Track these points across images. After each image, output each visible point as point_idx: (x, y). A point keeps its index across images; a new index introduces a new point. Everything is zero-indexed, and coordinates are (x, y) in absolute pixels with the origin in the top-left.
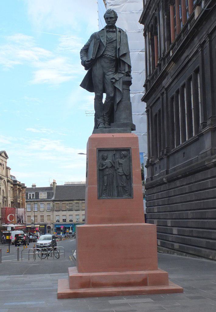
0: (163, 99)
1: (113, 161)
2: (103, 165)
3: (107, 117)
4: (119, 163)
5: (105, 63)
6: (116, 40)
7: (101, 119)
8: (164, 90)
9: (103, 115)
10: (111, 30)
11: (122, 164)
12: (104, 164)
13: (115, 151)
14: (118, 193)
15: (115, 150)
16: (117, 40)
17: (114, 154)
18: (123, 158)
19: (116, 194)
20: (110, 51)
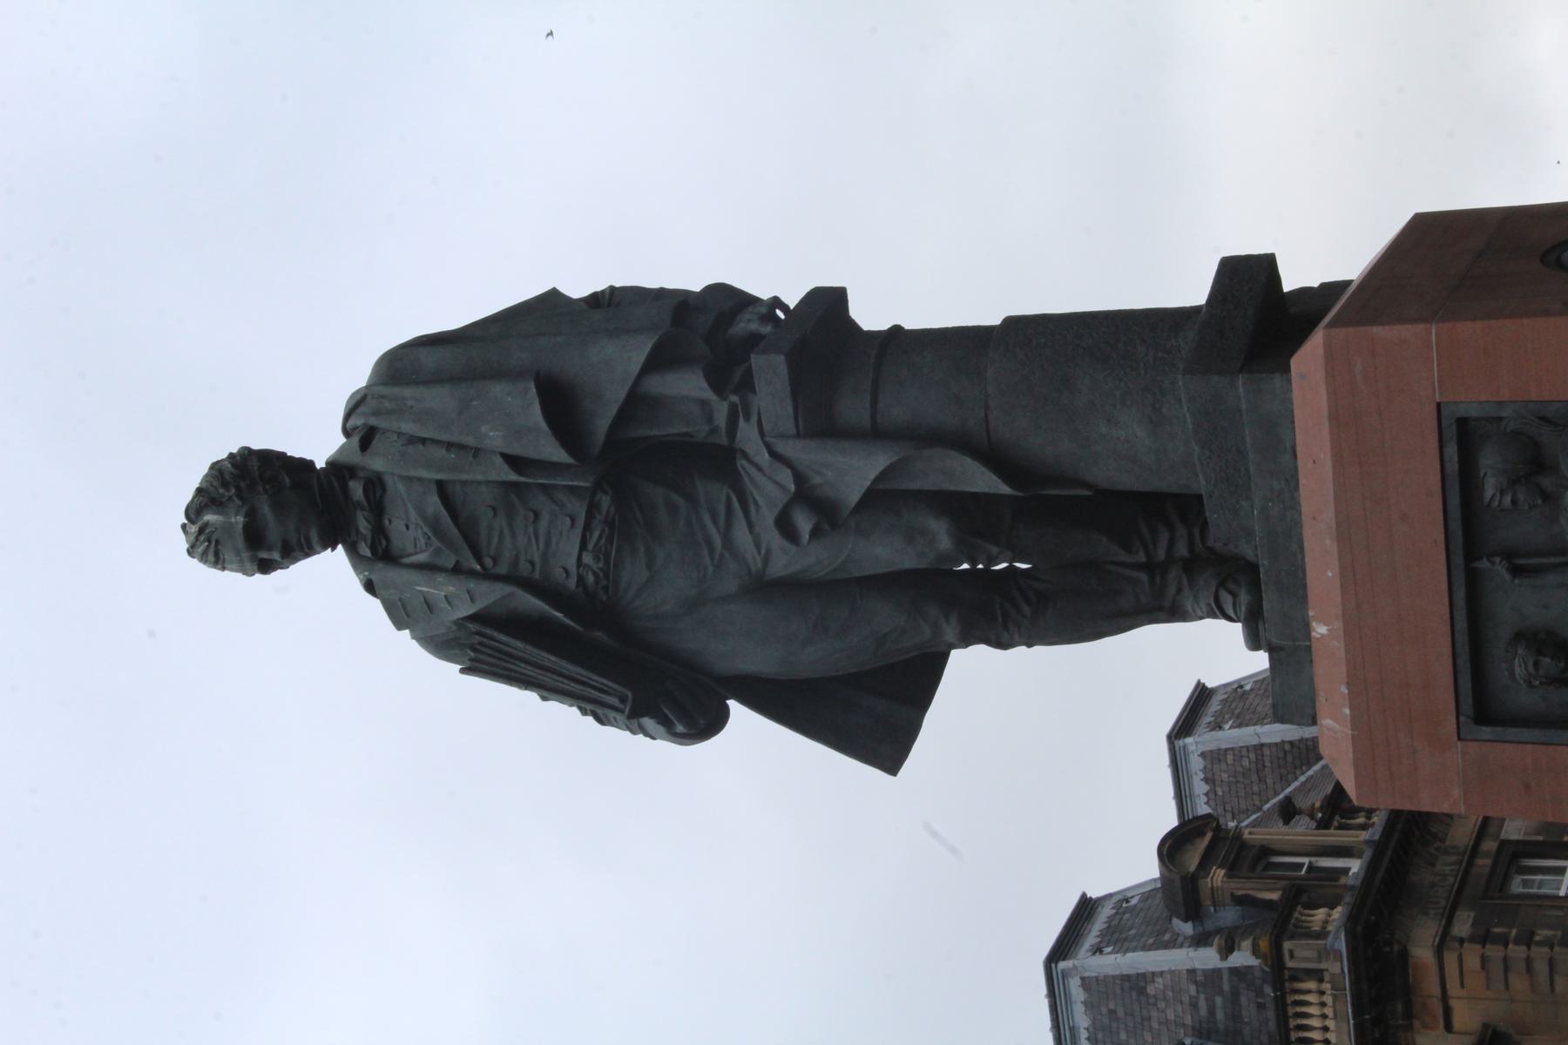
3: (1164, 538)
5: (658, 587)
6: (441, 486)
7: (1179, 591)
9: (1144, 577)
10: (363, 525)
15: (1471, 555)
16: (439, 477)
17: (1516, 571)
18: (1547, 482)
20: (548, 544)
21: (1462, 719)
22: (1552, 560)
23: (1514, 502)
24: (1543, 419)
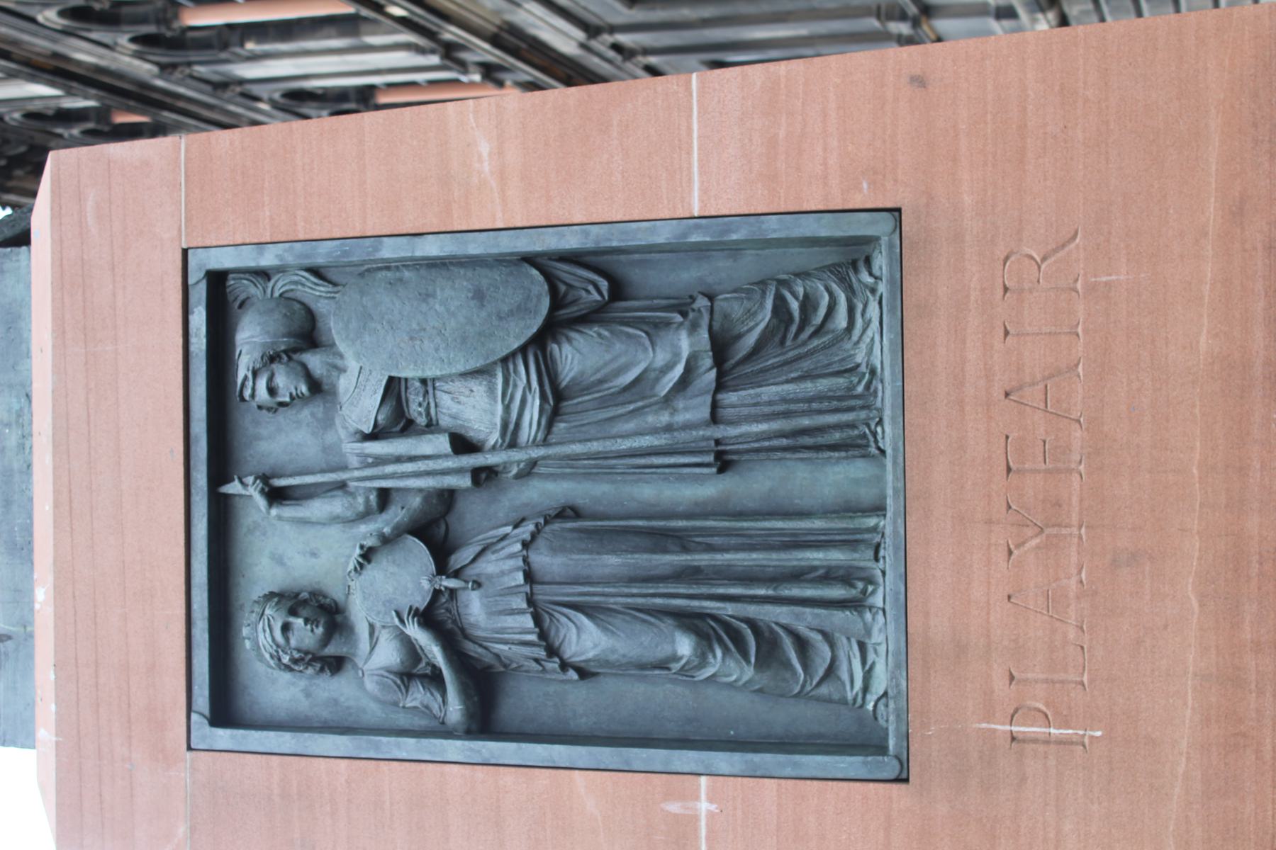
0: (647, 51)
1: (364, 516)
2: (413, 671)
4: (376, 434)
8: (594, 44)
11: (394, 389)
12: (388, 654)
13: (233, 488)
14: (805, 443)
19: (835, 478)
21: (194, 717)
22: (319, 478)
23: (272, 391)
24: (316, 271)
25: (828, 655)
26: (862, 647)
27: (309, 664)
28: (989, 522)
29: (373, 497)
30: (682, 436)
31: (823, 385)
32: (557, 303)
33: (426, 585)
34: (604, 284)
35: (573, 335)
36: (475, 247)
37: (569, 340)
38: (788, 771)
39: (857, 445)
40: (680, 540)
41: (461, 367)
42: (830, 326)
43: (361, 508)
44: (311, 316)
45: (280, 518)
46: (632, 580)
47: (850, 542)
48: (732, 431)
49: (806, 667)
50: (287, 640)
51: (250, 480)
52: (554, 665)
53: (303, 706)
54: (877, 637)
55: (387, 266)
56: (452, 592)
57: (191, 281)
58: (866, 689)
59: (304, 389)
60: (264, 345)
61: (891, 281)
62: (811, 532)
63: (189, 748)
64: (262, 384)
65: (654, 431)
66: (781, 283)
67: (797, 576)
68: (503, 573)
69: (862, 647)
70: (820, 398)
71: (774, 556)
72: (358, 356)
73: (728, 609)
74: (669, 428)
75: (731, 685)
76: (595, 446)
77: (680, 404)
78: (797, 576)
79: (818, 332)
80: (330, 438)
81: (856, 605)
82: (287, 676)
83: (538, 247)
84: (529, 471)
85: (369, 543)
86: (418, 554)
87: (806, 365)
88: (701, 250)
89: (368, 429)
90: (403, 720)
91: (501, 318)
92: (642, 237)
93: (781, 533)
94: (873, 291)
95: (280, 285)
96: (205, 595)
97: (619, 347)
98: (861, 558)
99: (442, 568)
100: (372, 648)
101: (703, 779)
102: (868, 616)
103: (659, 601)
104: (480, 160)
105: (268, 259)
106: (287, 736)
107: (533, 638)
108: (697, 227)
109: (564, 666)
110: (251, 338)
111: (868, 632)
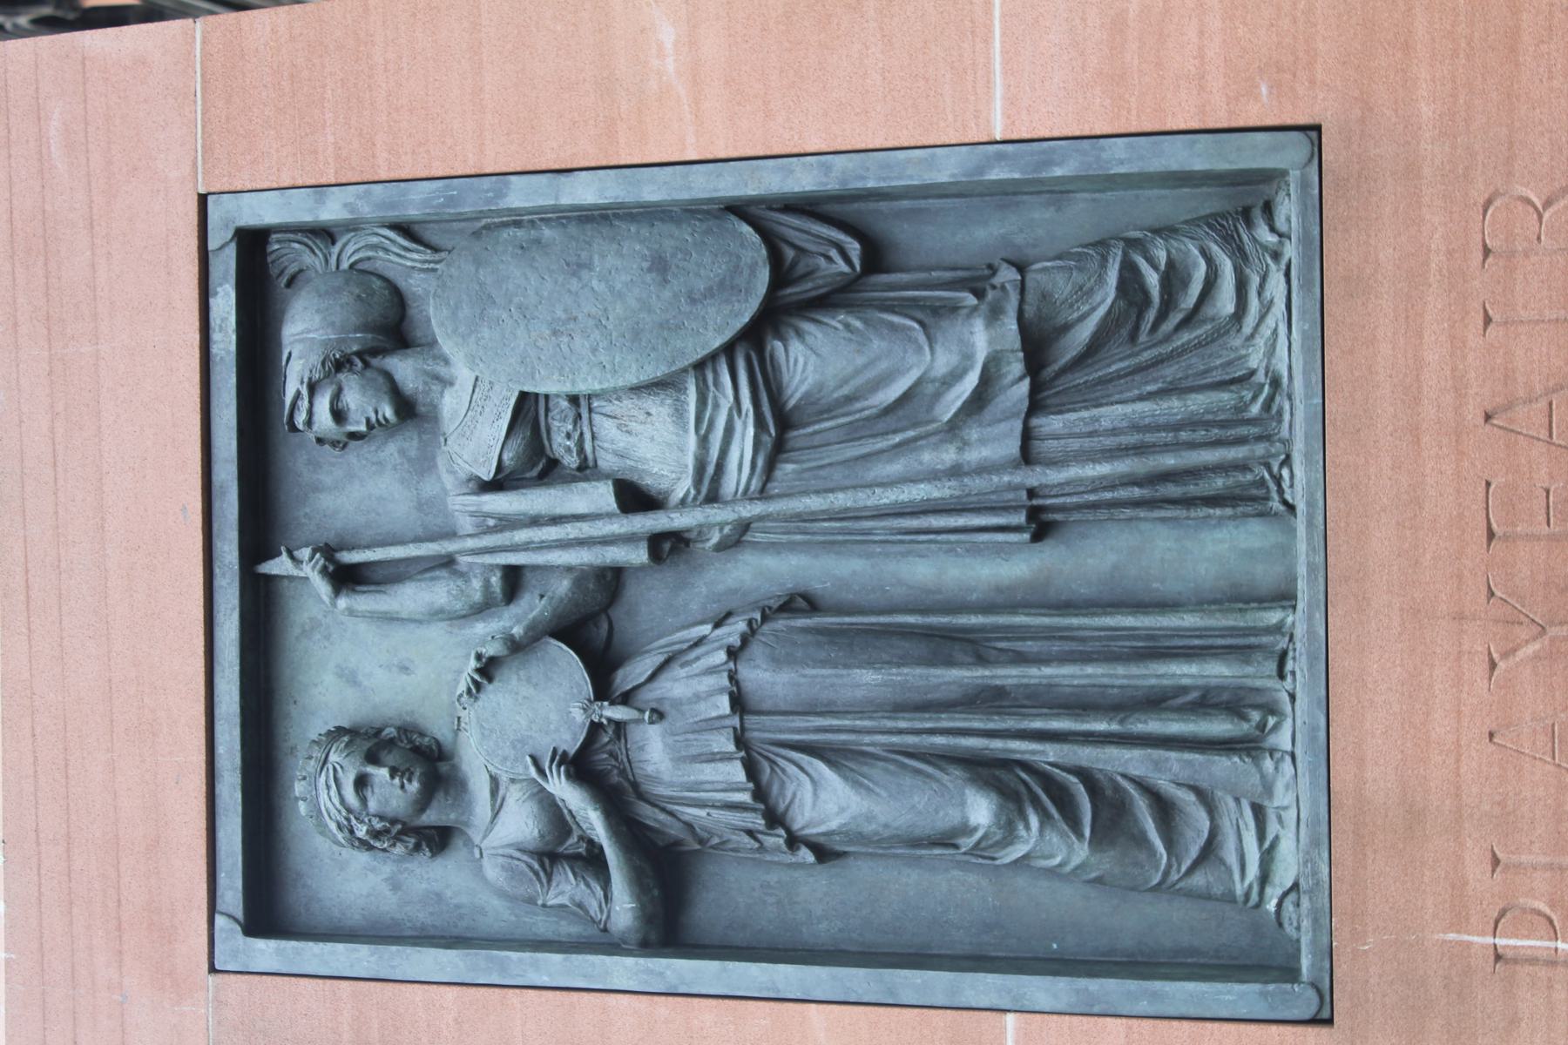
1: (482, 609)
2: (558, 850)
11: (527, 411)
12: (519, 823)
13: (279, 566)
14: (1168, 494)
19: (1216, 549)
21: (220, 921)
23: (339, 415)
24: (405, 229)
25: (1206, 825)
26: (1259, 812)
27: (397, 838)
28: (1460, 617)
29: (496, 580)
30: (977, 484)
31: (1198, 403)
32: (781, 275)
33: (579, 716)
34: (854, 248)
35: (807, 326)
36: (653, 189)
37: (800, 334)
38: (1143, 1007)
39: (1251, 497)
40: (974, 646)
41: (632, 378)
42: (1208, 311)
43: (478, 597)
44: (398, 299)
45: (351, 612)
46: (899, 708)
47: (1241, 651)
48: (1054, 476)
49: (1170, 844)
50: (364, 801)
51: (305, 553)
52: (777, 840)
53: (388, 904)
54: (1282, 797)
55: (517, 219)
56: (620, 727)
57: (212, 245)
58: (1264, 878)
59: (388, 411)
60: (325, 343)
61: (1305, 240)
62: (1178, 632)
63: (213, 970)
64: (323, 405)
65: (933, 476)
66: (1131, 243)
67: (1156, 701)
68: (698, 698)
69: (1259, 812)
70: (1192, 423)
71: (1121, 670)
72: (472, 360)
73: (1048, 754)
74: (956, 472)
75: (1052, 872)
76: (841, 500)
77: (974, 434)
78: (1156, 701)
79: (1188, 321)
80: (429, 488)
81: (1249, 746)
82: (363, 857)
83: (751, 190)
84: (738, 538)
85: (490, 650)
86: (565, 669)
87: (1170, 372)
88: (1006, 194)
89: (487, 473)
90: (543, 926)
91: (693, 301)
92: (914, 173)
93: (1131, 634)
94: (1276, 256)
95: (350, 250)
96: (237, 732)
97: (877, 344)
98: (1258, 674)
99: (603, 689)
100: (496, 815)
101: (1010, 1018)
102: (1268, 764)
103: (940, 740)
104: (661, 54)
105: (331, 210)
106: (363, 950)
107: (745, 797)
108: (1001, 157)
109: (793, 841)
110: (304, 333)
111: (1268, 789)
